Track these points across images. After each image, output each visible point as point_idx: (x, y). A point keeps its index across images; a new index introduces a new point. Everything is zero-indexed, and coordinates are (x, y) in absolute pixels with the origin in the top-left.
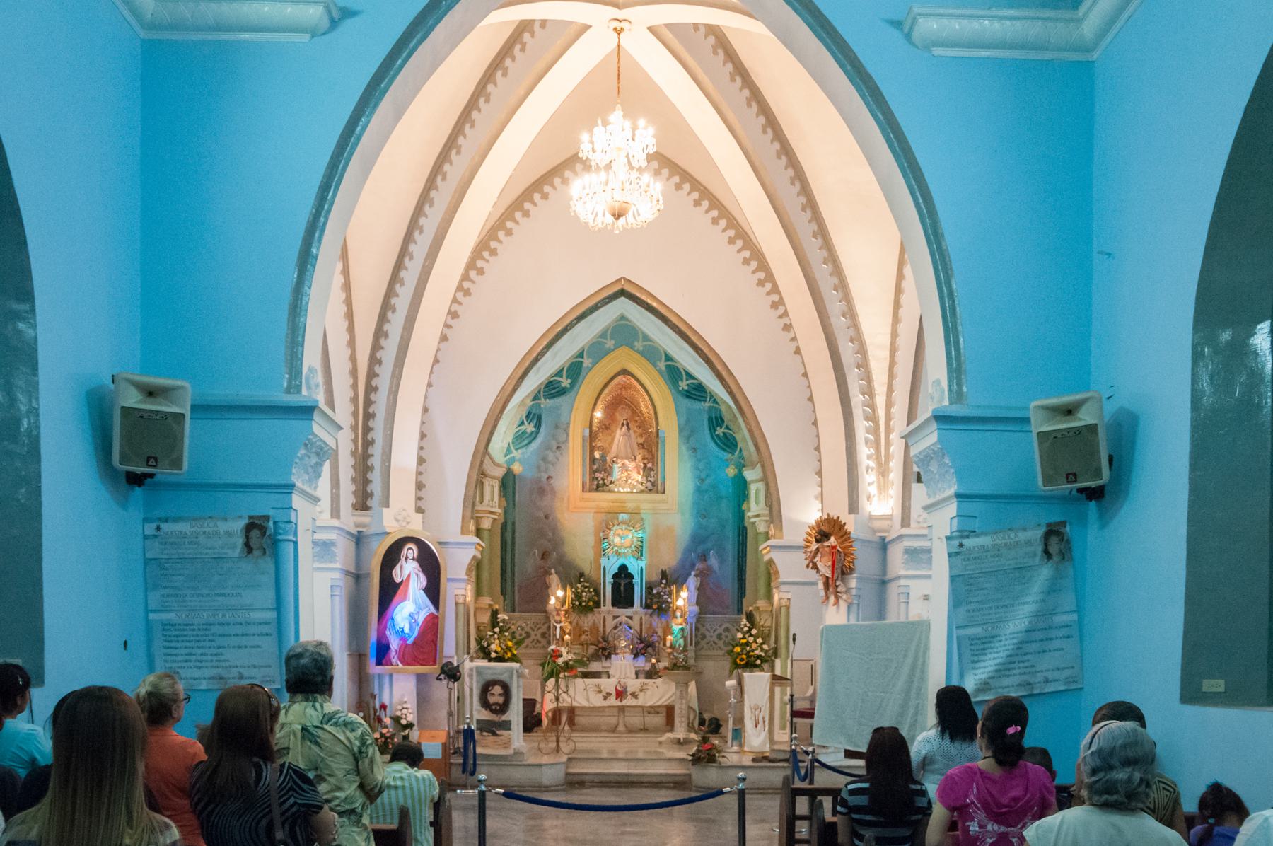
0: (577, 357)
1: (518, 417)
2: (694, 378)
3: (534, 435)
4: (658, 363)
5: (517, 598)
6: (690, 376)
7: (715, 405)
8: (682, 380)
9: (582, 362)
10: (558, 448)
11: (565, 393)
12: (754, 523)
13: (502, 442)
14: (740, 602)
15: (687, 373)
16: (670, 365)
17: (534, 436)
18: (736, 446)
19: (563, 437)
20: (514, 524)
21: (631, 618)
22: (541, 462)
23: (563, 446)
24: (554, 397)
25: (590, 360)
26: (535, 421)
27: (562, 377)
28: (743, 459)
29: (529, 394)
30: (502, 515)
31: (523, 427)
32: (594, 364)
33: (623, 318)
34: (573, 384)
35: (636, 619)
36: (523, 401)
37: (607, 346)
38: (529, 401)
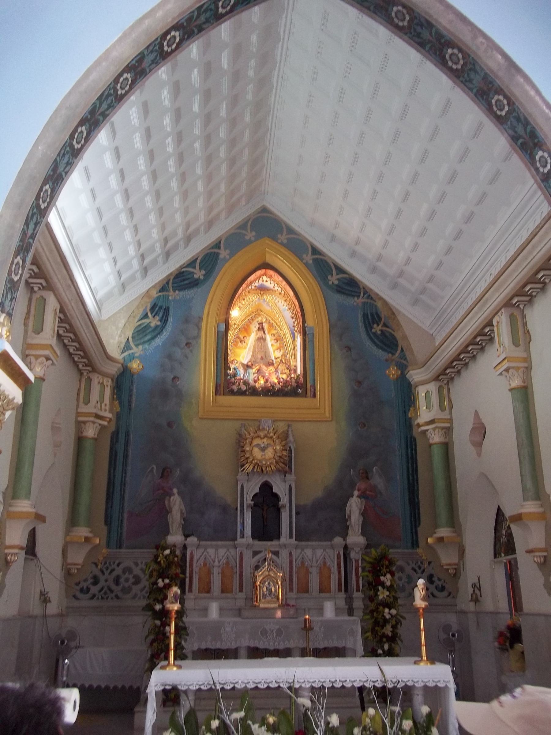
0: (212, 248)
3: (159, 330)
4: (304, 256)
5: (125, 529)
6: (340, 270)
7: (369, 301)
9: (218, 254)
10: (187, 344)
12: (424, 432)
13: (120, 336)
14: (414, 533)
16: (317, 259)
17: (158, 331)
18: (397, 346)
20: (127, 434)
21: (276, 553)
22: (167, 360)
24: (185, 289)
25: (228, 251)
26: (161, 314)
28: (405, 359)
29: (156, 284)
30: (113, 423)
31: (146, 321)
32: (232, 255)
33: (264, 210)
34: (208, 276)
35: (284, 554)
36: (147, 292)
37: (247, 238)
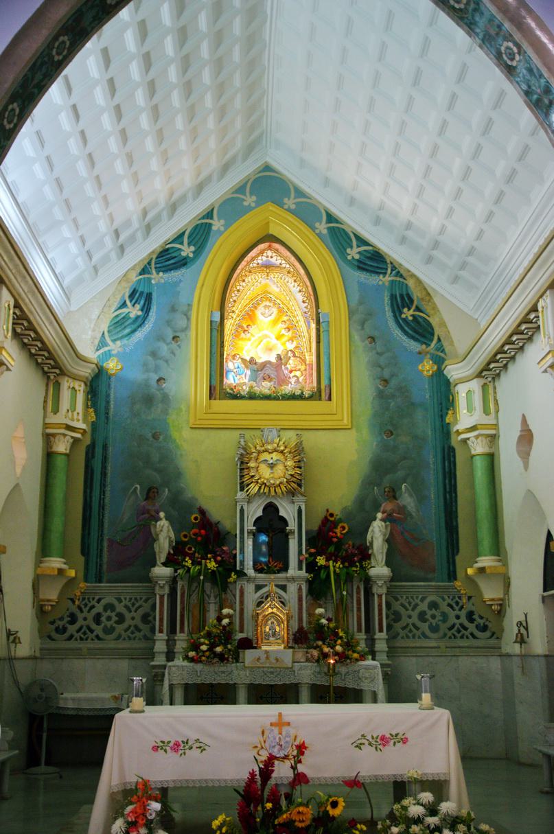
0: (203, 218)
1: (119, 297)
2: (368, 244)
3: (140, 321)
6: (362, 242)
8: (352, 247)
9: (210, 225)
11: (185, 264)
15: (358, 238)
19: (182, 323)
20: (105, 447)
22: (150, 358)
23: (182, 335)
24: (171, 270)
26: (142, 302)
27: (182, 243)
31: (125, 310)
32: (227, 227)
34: (197, 253)
38: (135, 275)
